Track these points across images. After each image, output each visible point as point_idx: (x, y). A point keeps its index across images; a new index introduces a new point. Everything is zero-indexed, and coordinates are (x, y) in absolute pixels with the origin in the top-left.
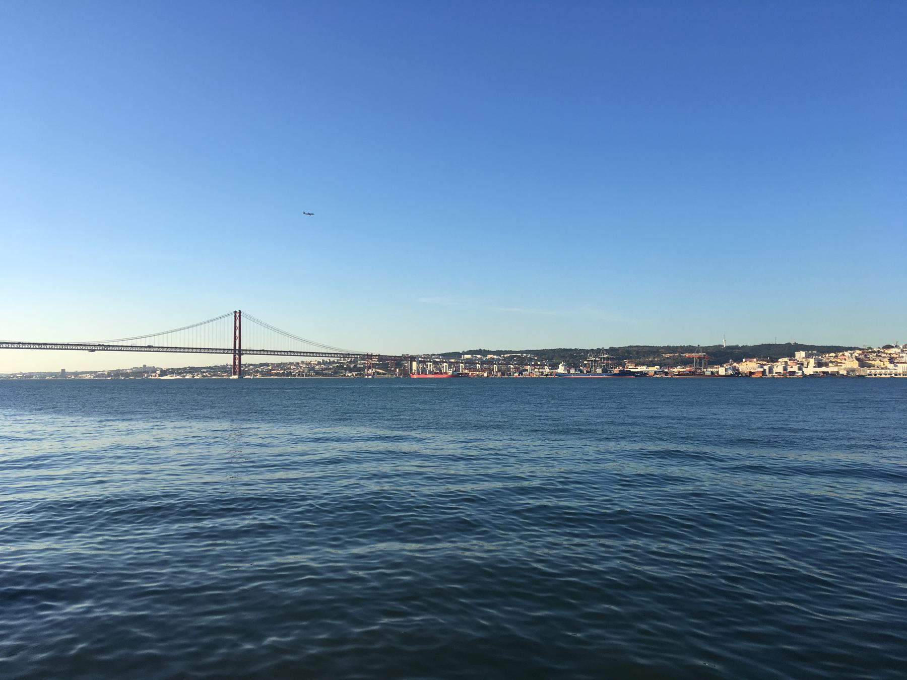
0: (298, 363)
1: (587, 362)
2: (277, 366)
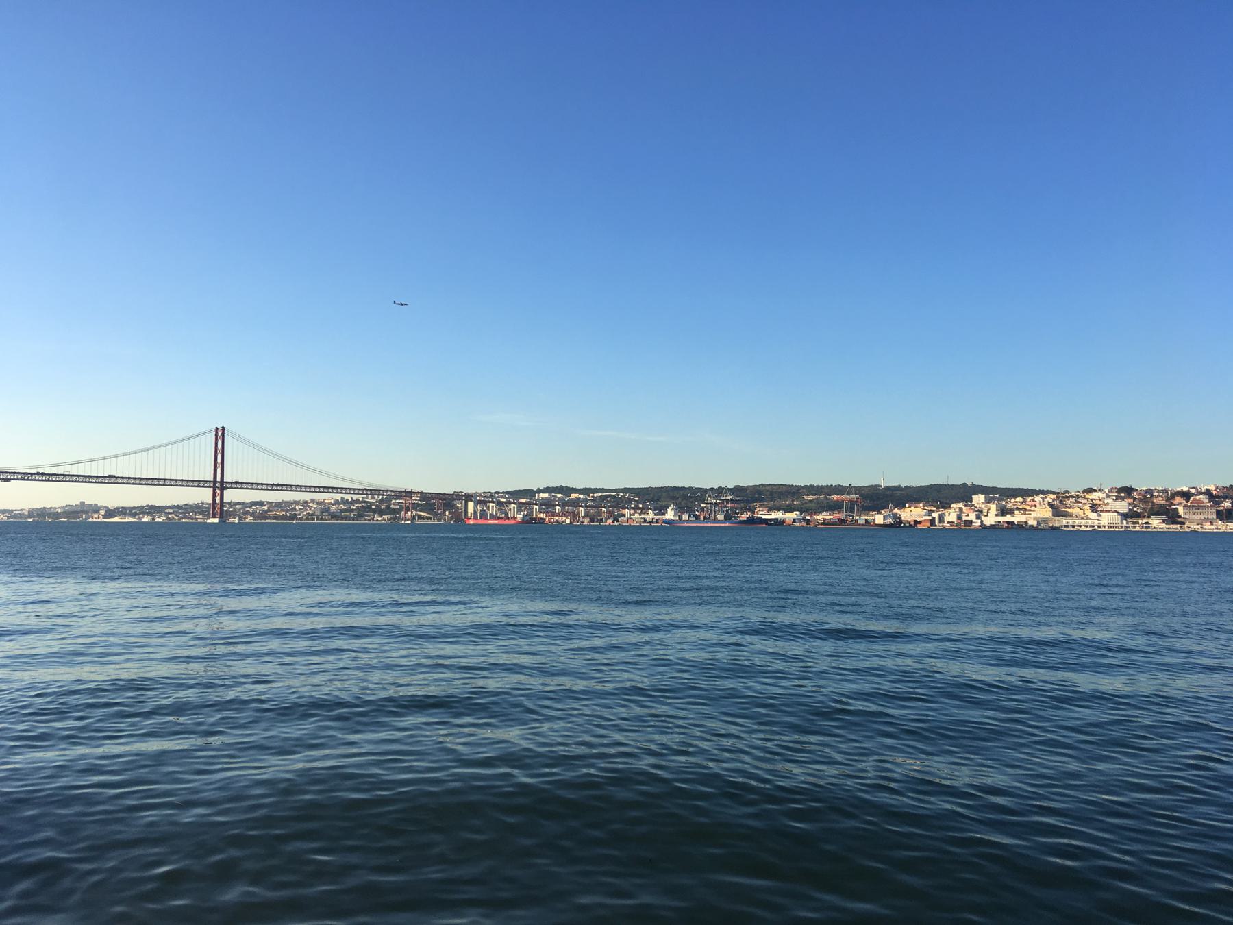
0: (306, 502)
1: (704, 505)
2: (275, 506)
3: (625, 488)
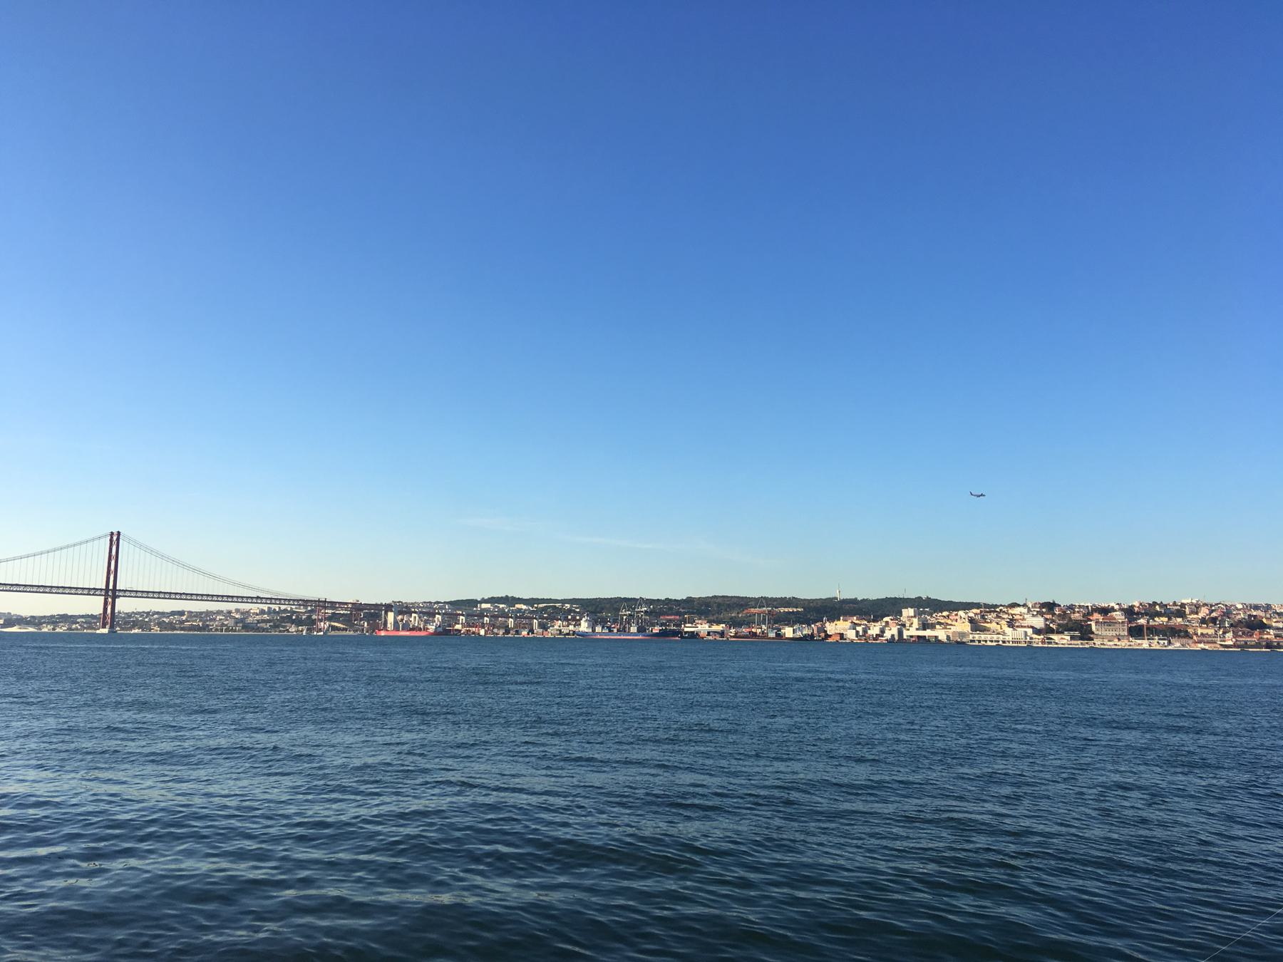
0: (230, 612)
2: (194, 616)
3: (574, 599)
